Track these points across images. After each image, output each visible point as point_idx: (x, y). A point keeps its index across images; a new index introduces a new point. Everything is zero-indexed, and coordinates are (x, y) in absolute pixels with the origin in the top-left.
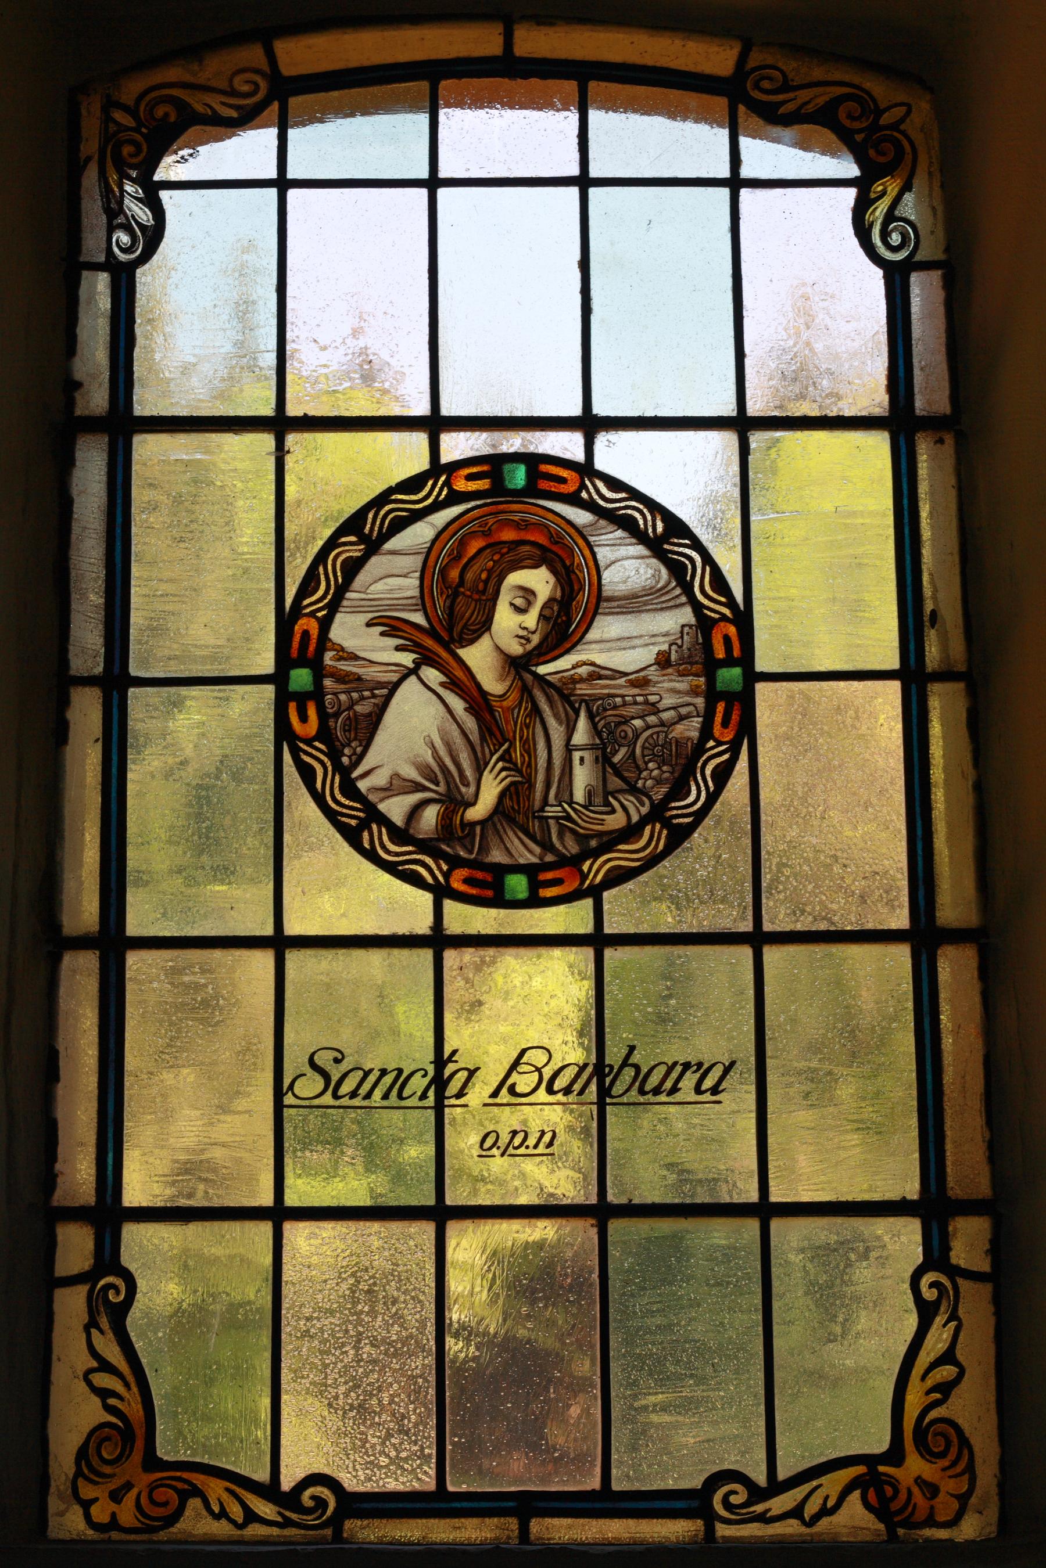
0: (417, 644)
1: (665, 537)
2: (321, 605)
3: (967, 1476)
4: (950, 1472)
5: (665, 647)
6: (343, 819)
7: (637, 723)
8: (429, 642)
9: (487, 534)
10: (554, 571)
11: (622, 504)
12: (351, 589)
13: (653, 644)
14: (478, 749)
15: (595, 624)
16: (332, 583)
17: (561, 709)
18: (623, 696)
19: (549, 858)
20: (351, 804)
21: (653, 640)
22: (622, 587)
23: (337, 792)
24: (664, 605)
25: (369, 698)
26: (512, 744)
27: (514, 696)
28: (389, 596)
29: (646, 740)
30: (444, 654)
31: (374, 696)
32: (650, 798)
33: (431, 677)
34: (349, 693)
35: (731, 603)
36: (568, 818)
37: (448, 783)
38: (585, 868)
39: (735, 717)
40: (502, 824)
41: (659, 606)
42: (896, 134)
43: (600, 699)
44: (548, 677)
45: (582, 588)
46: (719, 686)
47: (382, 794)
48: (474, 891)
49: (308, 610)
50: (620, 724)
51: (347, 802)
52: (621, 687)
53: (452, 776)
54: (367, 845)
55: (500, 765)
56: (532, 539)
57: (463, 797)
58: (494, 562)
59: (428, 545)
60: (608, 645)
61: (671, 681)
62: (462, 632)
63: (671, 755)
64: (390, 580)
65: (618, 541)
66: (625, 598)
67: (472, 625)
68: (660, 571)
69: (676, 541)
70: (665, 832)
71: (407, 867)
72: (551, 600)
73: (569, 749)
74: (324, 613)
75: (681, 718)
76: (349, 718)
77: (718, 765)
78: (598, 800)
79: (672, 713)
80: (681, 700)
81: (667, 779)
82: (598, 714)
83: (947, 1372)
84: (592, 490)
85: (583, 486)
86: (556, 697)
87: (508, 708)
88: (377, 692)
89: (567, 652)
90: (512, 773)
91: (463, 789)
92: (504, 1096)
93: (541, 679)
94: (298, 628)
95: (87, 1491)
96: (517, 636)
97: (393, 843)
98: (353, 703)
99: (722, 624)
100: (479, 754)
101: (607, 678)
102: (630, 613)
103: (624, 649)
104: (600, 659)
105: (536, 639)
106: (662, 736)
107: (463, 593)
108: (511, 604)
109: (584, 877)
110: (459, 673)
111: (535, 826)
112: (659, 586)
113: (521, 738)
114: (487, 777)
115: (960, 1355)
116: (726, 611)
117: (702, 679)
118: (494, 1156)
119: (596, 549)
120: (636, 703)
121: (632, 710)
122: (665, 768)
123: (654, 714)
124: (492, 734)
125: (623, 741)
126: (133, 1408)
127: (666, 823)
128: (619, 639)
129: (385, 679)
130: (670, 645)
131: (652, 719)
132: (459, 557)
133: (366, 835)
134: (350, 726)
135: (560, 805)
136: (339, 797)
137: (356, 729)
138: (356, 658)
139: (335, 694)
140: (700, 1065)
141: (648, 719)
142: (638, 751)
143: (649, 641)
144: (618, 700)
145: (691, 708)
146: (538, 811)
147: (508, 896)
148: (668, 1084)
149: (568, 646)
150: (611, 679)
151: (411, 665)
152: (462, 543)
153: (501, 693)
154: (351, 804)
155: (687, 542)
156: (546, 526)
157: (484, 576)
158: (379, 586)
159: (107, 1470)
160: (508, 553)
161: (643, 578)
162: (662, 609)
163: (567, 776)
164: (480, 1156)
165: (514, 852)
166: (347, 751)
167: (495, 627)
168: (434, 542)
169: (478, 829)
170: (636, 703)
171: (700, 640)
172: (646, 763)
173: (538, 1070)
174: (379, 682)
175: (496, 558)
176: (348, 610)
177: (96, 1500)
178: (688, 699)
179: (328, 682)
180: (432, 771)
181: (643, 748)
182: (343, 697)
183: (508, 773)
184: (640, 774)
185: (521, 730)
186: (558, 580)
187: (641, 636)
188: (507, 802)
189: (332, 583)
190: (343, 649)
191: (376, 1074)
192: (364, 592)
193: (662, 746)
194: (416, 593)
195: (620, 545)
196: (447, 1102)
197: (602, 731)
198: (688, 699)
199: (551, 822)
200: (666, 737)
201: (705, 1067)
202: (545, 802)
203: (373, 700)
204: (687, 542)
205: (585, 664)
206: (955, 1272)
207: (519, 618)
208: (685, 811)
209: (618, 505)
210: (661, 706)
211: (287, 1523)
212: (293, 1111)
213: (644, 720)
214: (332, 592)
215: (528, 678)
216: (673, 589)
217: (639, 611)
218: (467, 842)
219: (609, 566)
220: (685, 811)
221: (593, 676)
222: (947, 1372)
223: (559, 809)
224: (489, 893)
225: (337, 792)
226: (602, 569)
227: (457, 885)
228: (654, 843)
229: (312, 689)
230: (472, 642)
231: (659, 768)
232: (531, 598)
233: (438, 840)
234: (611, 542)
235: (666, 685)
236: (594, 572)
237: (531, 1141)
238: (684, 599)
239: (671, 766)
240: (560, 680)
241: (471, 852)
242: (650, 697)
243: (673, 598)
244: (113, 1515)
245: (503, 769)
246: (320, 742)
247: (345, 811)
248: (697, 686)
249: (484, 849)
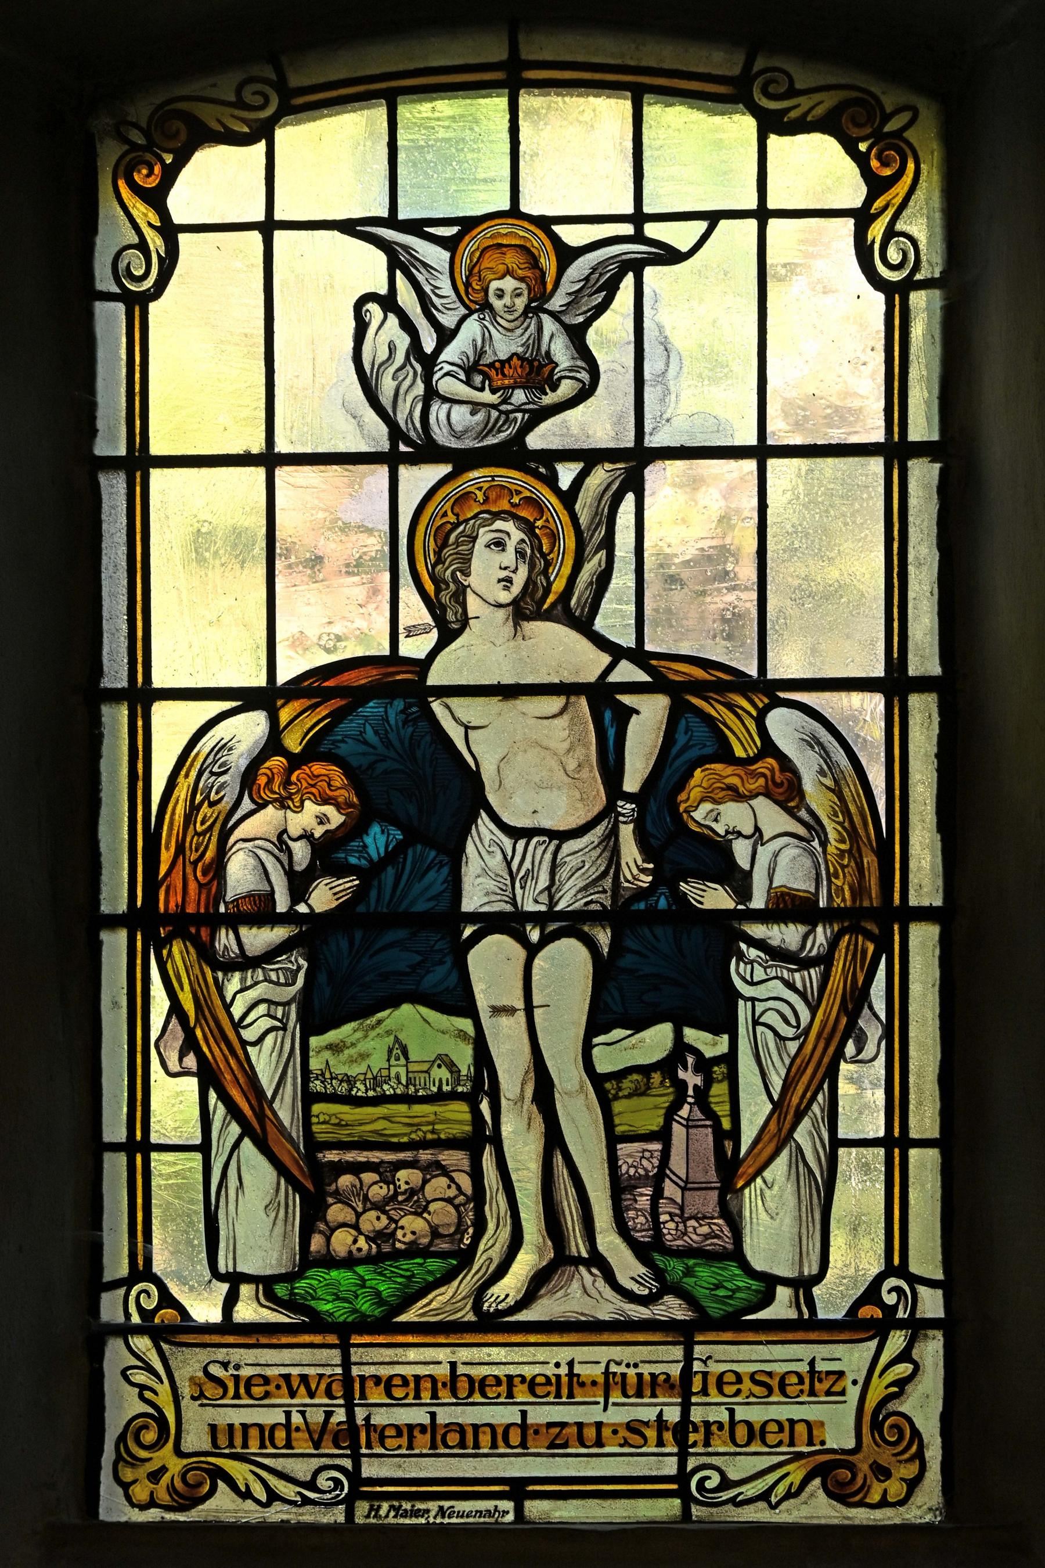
83: (903, 1369)
95: (128, 1475)
115: (915, 1354)
159: (143, 1454)
177: (135, 1481)
206: (914, 1280)
211: (306, 1501)
222: (903, 1369)
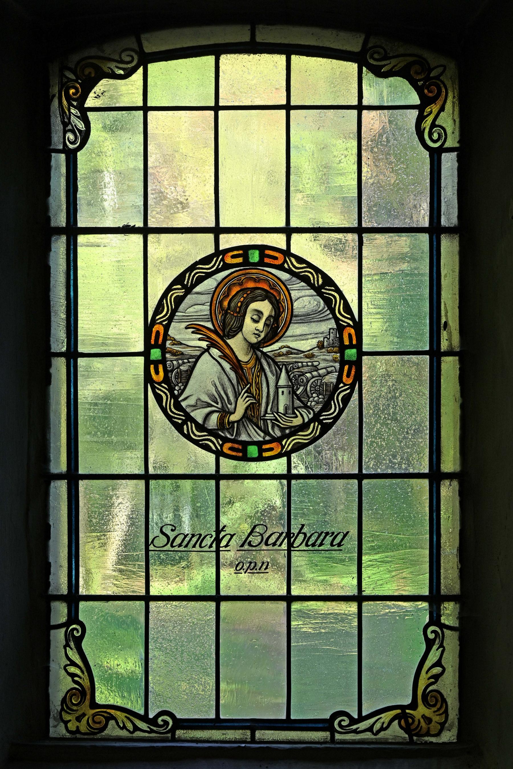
0: (209, 337)
1: (323, 286)
3: (444, 715)
4: (437, 713)
5: (322, 339)
6: (175, 420)
7: (308, 375)
8: (214, 336)
9: (241, 284)
10: (271, 302)
11: (303, 270)
13: (316, 338)
14: (236, 387)
15: (290, 328)
17: (274, 368)
18: (302, 363)
19: (267, 438)
20: (179, 413)
21: (316, 336)
22: (302, 310)
23: (172, 407)
24: (322, 319)
25: (187, 363)
26: (251, 385)
27: (253, 362)
28: (195, 314)
29: (312, 383)
30: (221, 342)
31: (189, 362)
32: (313, 410)
33: (215, 353)
34: (178, 360)
35: (353, 318)
36: (276, 420)
37: (222, 403)
38: (284, 443)
40: (246, 423)
41: (319, 319)
42: (438, 81)
43: (292, 363)
44: (268, 353)
45: (284, 310)
46: (346, 358)
47: (193, 408)
48: (234, 454)
50: (299, 376)
51: (177, 412)
52: (301, 358)
53: (224, 400)
54: (186, 432)
55: (246, 395)
56: (261, 287)
57: (229, 410)
58: (244, 298)
59: (214, 290)
60: (296, 338)
61: (324, 355)
62: (229, 332)
63: (323, 390)
65: (301, 288)
66: (304, 315)
67: (233, 328)
68: (320, 302)
69: (328, 288)
70: (320, 426)
72: (270, 316)
73: (277, 387)
75: (328, 373)
76: (178, 372)
77: (345, 395)
78: (290, 411)
79: (324, 371)
80: (328, 364)
81: (321, 402)
82: (291, 371)
84: (289, 263)
85: (285, 261)
86: (272, 363)
87: (250, 368)
88: (190, 360)
89: (277, 341)
90: (252, 398)
91: (229, 406)
93: (264, 354)
95: (66, 717)
96: (254, 334)
97: (198, 431)
98: (179, 365)
99: (348, 328)
100: (236, 390)
101: (295, 354)
102: (306, 322)
103: (303, 340)
104: (293, 345)
105: (263, 335)
106: (319, 382)
107: (230, 313)
108: (252, 318)
109: (283, 447)
110: (227, 351)
111: (261, 423)
112: (319, 310)
113: (255, 382)
114: (240, 400)
116: (351, 323)
117: (339, 354)
119: (291, 292)
120: (308, 366)
121: (306, 369)
122: (320, 397)
123: (316, 371)
124: (242, 380)
125: (301, 384)
126: (86, 683)
127: (320, 422)
128: (300, 335)
129: (194, 354)
130: (324, 338)
131: (315, 373)
132: (228, 295)
133: (185, 427)
134: (178, 376)
135: (273, 414)
136: (173, 410)
137: (181, 378)
138: (181, 344)
139: (171, 361)
140: (333, 533)
141: (313, 373)
142: (308, 388)
143: (315, 336)
144: (300, 364)
145: (333, 368)
146: (263, 417)
147: (249, 456)
148: (319, 542)
149: (277, 338)
150: (297, 354)
151: (206, 348)
152: (229, 289)
153: (246, 361)
154: (179, 413)
155: (333, 288)
156: (268, 280)
157: (239, 304)
160: (250, 293)
161: (312, 306)
162: (320, 321)
163: (276, 399)
165: (251, 435)
166: (177, 388)
167: (244, 329)
168: (216, 288)
169: (236, 425)
170: (308, 366)
171: (338, 336)
172: (312, 394)
174: (191, 355)
175: (245, 296)
178: (331, 364)
179: (168, 356)
180: (215, 397)
181: (311, 387)
182: (175, 362)
183: (249, 398)
184: (309, 399)
185: (255, 378)
186: (273, 307)
187: (311, 334)
188: (249, 412)
190: (175, 340)
193: (319, 386)
194: (208, 313)
195: (302, 290)
196: (221, 549)
197: (292, 379)
198: (331, 364)
199: (269, 421)
200: (321, 382)
201: (335, 534)
202: (266, 412)
203: (188, 364)
204: (333, 288)
205: (285, 347)
207: (256, 325)
208: (329, 417)
209: (301, 270)
210: (319, 367)
213: (311, 374)
215: (259, 353)
216: (326, 311)
217: (310, 322)
218: (231, 431)
219: (297, 300)
220: (329, 417)
221: (288, 353)
223: (272, 415)
224: (240, 454)
225: (172, 407)
226: (293, 301)
227: (226, 450)
228: (314, 432)
229: (161, 358)
230: (234, 336)
231: (318, 396)
232: (261, 315)
233: (217, 430)
234: (298, 288)
235: (322, 357)
236: (289, 303)
238: (331, 316)
239: (323, 395)
240: (273, 355)
241: (232, 436)
242: (314, 363)
243: (326, 316)
244: (78, 727)
245: (247, 397)
247: (176, 416)
248: (336, 358)
249: (238, 434)
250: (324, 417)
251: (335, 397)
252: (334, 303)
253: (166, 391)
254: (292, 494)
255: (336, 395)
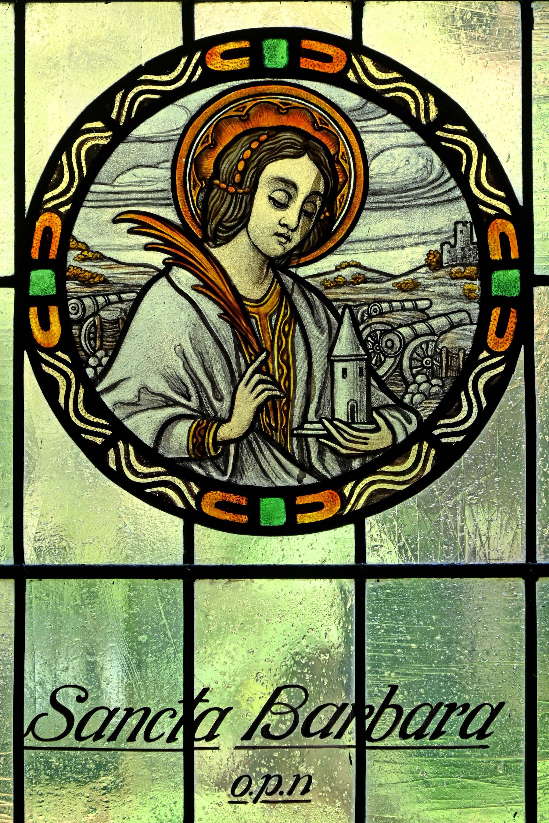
0: (168, 243)
1: (438, 124)
2: (64, 199)
5: (437, 247)
6: (88, 437)
7: (405, 331)
8: (180, 240)
9: (244, 119)
10: (317, 162)
11: (392, 86)
12: (96, 180)
13: (423, 243)
14: (233, 359)
15: (361, 221)
16: (76, 174)
17: (323, 316)
18: (390, 302)
19: (308, 480)
20: (97, 420)
21: (423, 238)
22: (390, 179)
23: (81, 406)
24: (436, 200)
25: (115, 302)
26: (270, 354)
27: (273, 300)
28: (137, 189)
29: (415, 350)
30: (198, 255)
31: (121, 301)
32: (417, 414)
33: (183, 280)
34: (94, 297)
35: (510, 199)
36: (330, 436)
37: (200, 398)
38: (347, 491)
39: (511, 325)
40: (258, 443)
41: (431, 201)
43: (365, 304)
44: (309, 280)
45: (347, 180)
46: (495, 291)
47: (130, 409)
48: (228, 517)
49: (49, 205)
50: (384, 333)
51: (92, 418)
52: (388, 290)
53: (205, 389)
54: (113, 465)
55: (257, 377)
56: (293, 124)
57: (216, 413)
58: (252, 150)
59: (180, 132)
60: (374, 244)
61: (442, 284)
62: (216, 229)
63: (441, 367)
64: (138, 171)
65: (388, 128)
66: (394, 191)
67: (227, 221)
68: (432, 161)
69: (450, 127)
70: (433, 452)
71: (155, 489)
72: (314, 193)
73: (331, 360)
74: (68, 207)
75: (453, 326)
76: (94, 325)
77: (492, 378)
78: (362, 416)
79: (443, 320)
80: (453, 306)
81: (436, 394)
82: (363, 321)
84: (360, 70)
85: (350, 65)
86: (318, 302)
87: (266, 315)
88: (124, 296)
89: (331, 251)
90: (270, 386)
91: (216, 404)
92: (258, 739)
93: (300, 282)
94: (39, 225)
96: (276, 234)
97: (141, 463)
98: (98, 309)
99: (499, 221)
100: (234, 366)
101: (373, 281)
102: (399, 208)
103: (392, 249)
104: (367, 260)
105: (296, 237)
106: (432, 346)
107: (218, 186)
108: (270, 198)
109: (345, 501)
110: (213, 275)
111: (293, 445)
112: (431, 178)
113: (279, 348)
114: (243, 391)
116: (506, 209)
117: (477, 283)
118: (246, 803)
119: (363, 136)
120: (404, 309)
121: (399, 317)
122: (434, 381)
123: (424, 321)
124: (248, 343)
125: (389, 351)
127: (434, 442)
128: (386, 238)
129: (134, 282)
130: (442, 244)
131: (421, 327)
132: (214, 145)
133: (111, 453)
134: (95, 334)
135: (321, 422)
136: (83, 412)
137: (102, 337)
138: (103, 258)
139: (79, 298)
140: (466, 706)
141: (416, 326)
143: (417, 241)
144: (385, 306)
145: (464, 315)
146: (296, 429)
147: (263, 523)
148: (432, 728)
149: (330, 245)
150: (378, 282)
151: (162, 267)
152: (218, 130)
153: (258, 298)
154: (97, 420)
155: (463, 128)
156: (308, 110)
157: (241, 166)
158: (127, 178)
160: (267, 140)
161: (414, 170)
162: (434, 204)
163: (329, 388)
164: (230, 802)
165: (270, 473)
166: (92, 361)
167: (252, 224)
168: (187, 127)
169: (232, 448)
170: (404, 309)
171: (475, 239)
172: (414, 376)
173: (294, 710)
174: (126, 285)
175: (254, 145)
176: (93, 204)
178: (460, 305)
179: (71, 285)
180: (184, 384)
181: (411, 359)
182: (88, 302)
183: (265, 386)
184: (407, 388)
185: (280, 338)
186: (321, 171)
187: (411, 234)
188: (264, 419)
189: (76, 174)
190: (88, 248)
191: (122, 713)
192: (111, 185)
193: (432, 357)
194: (167, 185)
195: (389, 132)
197: (366, 340)
198: (460, 305)
199: (311, 440)
200: (436, 346)
201: (472, 708)
202: (304, 419)
203: (120, 305)
204: (463, 128)
205: (349, 265)
207: (280, 214)
208: (455, 429)
209: (387, 86)
210: (431, 312)
212: (32, 753)
213: (413, 328)
214: (76, 184)
215: (288, 281)
216: (446, 181)
217: (409, 207)
218: (220, 462)
219: (377, 155)
220: (455, 429)
221: (358, 280)
223: (320, 426)
224: (244, 519)
225: (81, 406)
226: (369, 159)
227: (208, 509)
228: (421, 464)
229: (54, 292)
230: (227, 240)
231: (428, 381)
232: (292, 191)
233: (189, 460)
234: (380, 128)
235: (437, 289)
236: (360, 162)
237: (285, 788)
238: (458, 193)
239: (441, 379)
240: (322, 284)
241: (224, 474)
242: (419, 303)
243: (446, 192)
245: (260, 382)
246: (63, 352)
247: (89, 428)
248: (471, 291)
249: (238, 470)
250: (444, 430)
251: (470, 384)
252: (465, 162)
253: (65, 368)
254: (368, 612)
255: (471, 378)
